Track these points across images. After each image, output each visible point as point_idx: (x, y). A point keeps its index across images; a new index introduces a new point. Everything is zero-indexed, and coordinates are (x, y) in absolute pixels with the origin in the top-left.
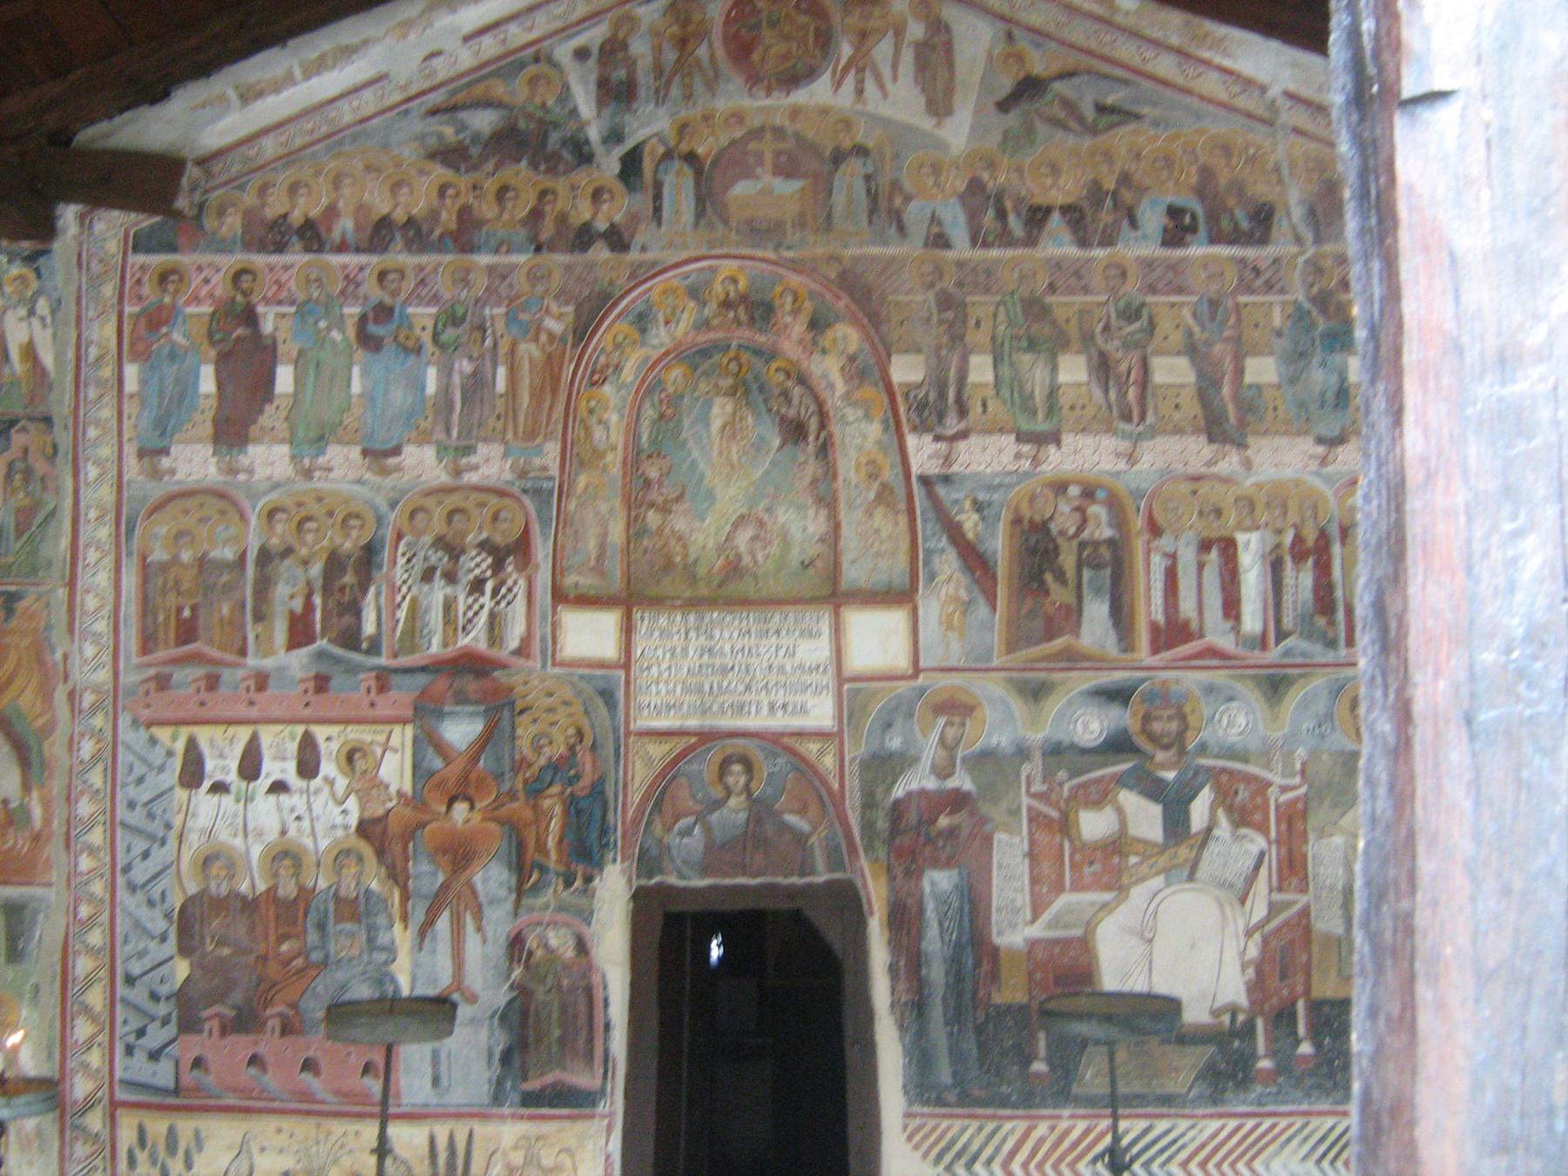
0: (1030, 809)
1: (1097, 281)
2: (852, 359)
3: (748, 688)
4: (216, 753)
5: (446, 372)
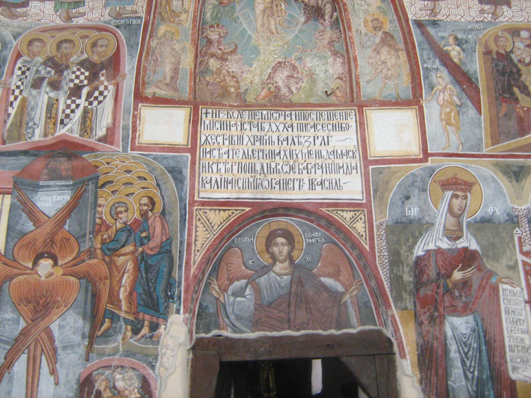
0: (524, 263)
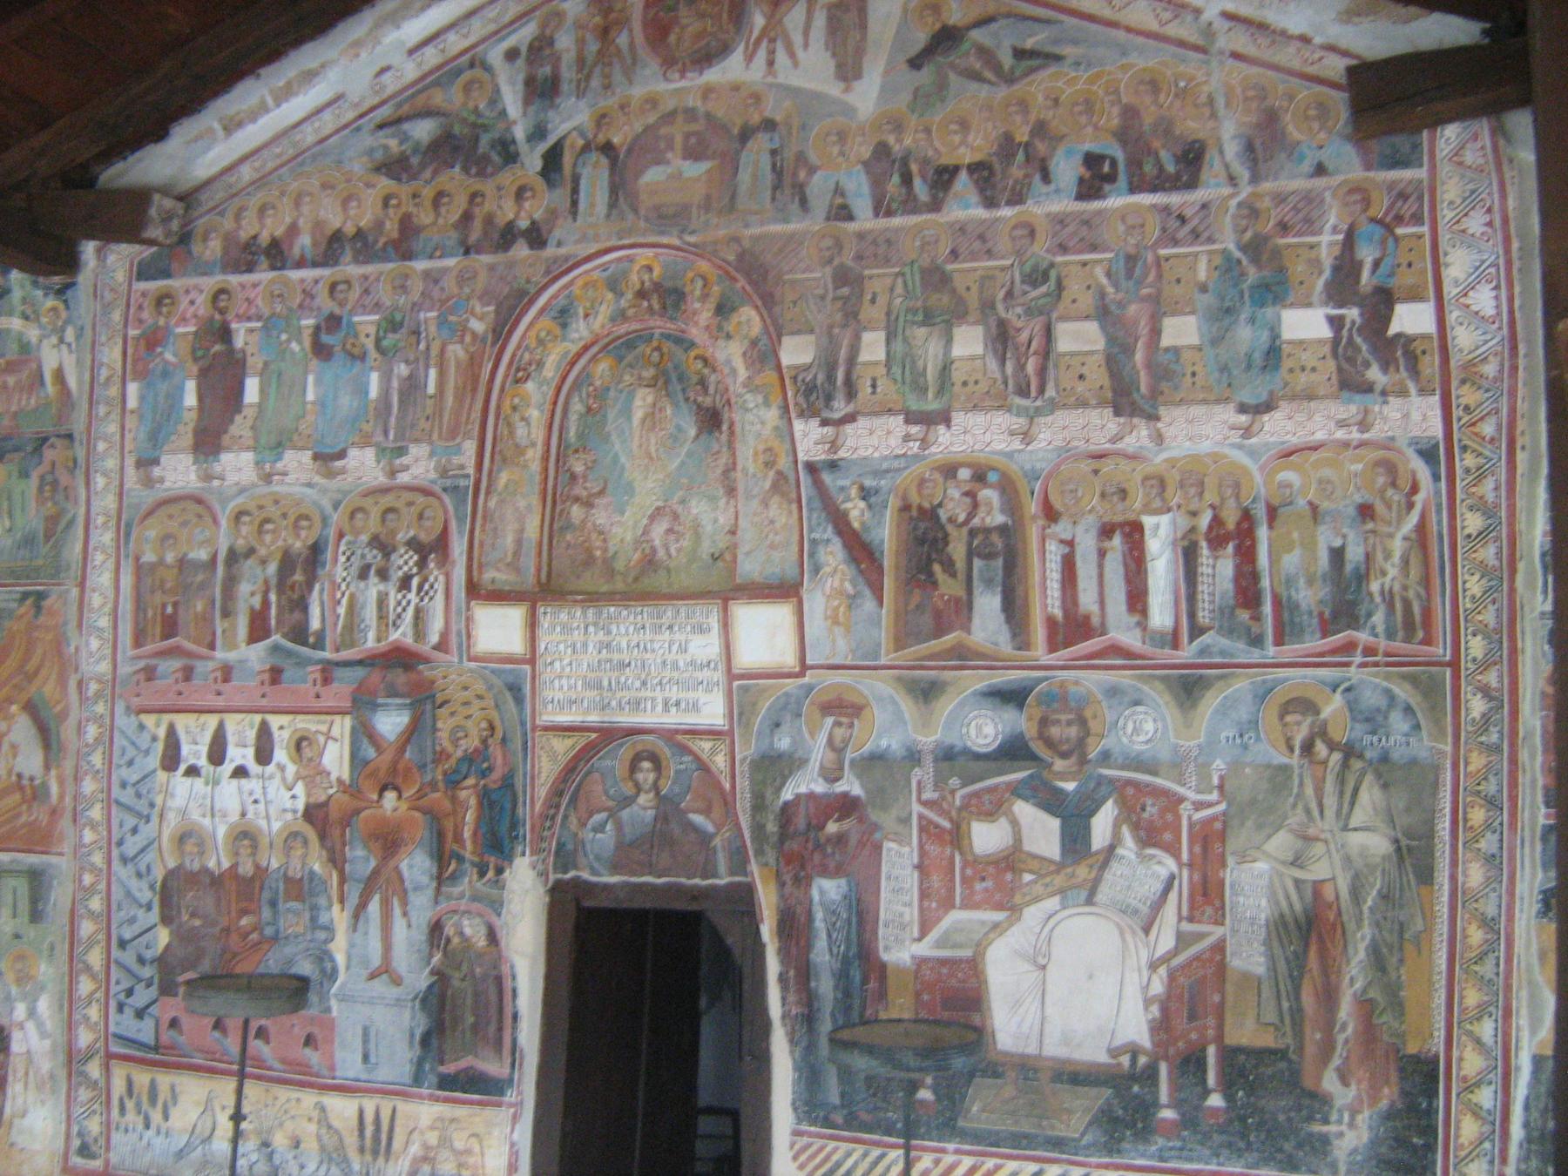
0: (921, 817)
1: (1003, 244)
2: (754, 343)
3: (644, 683)
5: (386, 378)
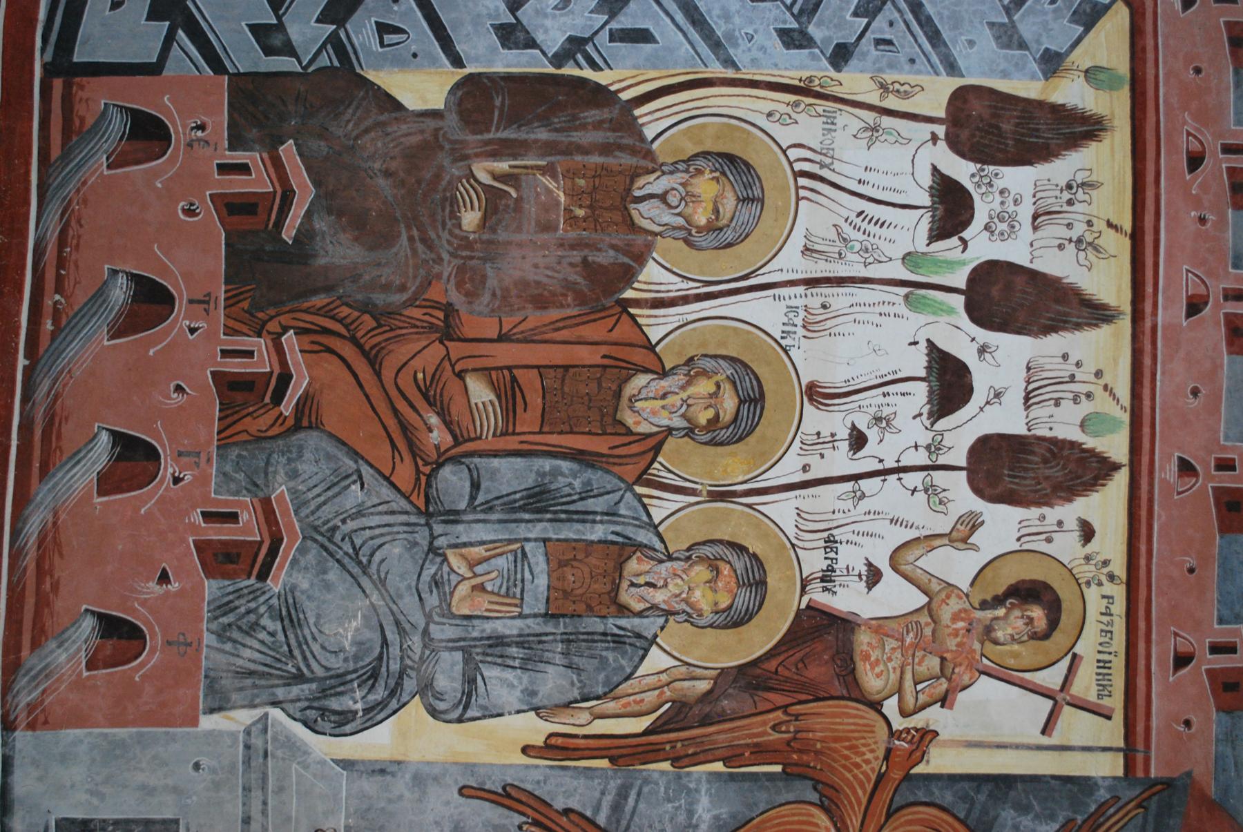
4: (1056, 200)
